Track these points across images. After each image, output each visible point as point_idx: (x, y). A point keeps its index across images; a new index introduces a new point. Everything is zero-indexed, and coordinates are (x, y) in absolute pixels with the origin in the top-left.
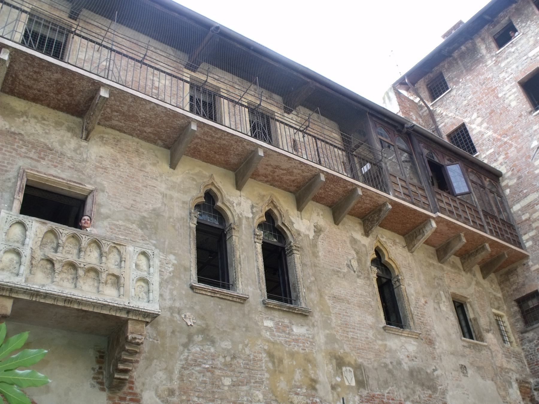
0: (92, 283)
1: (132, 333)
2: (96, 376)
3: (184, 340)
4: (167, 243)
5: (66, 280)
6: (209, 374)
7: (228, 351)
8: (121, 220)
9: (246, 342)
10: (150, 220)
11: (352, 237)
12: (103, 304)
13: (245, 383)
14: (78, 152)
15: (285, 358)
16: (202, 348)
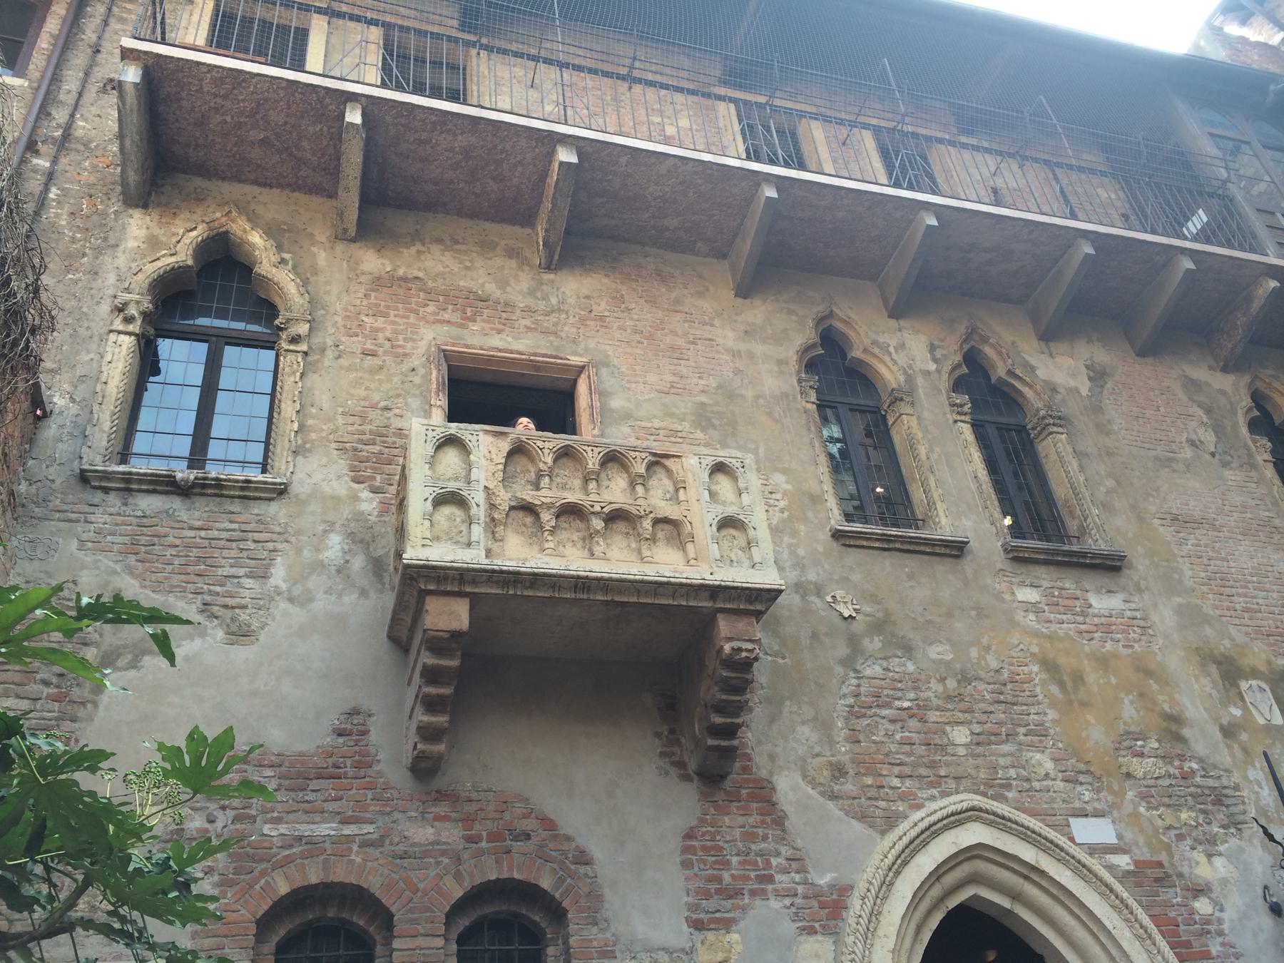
0: (625, 543)
1: (730, 639)
2: (665, 749)
3: (843, 650)
4: (762, 450)
5: (571, 544)
6: (913, 723)
7: (947, 664)
8: (655, 417)
9: (985, 641)
10: (716, 409)
11: (1186, 377)
12: (656, 583)
14: (539, 294)
15: (1088, 669)
16: (885, 665)
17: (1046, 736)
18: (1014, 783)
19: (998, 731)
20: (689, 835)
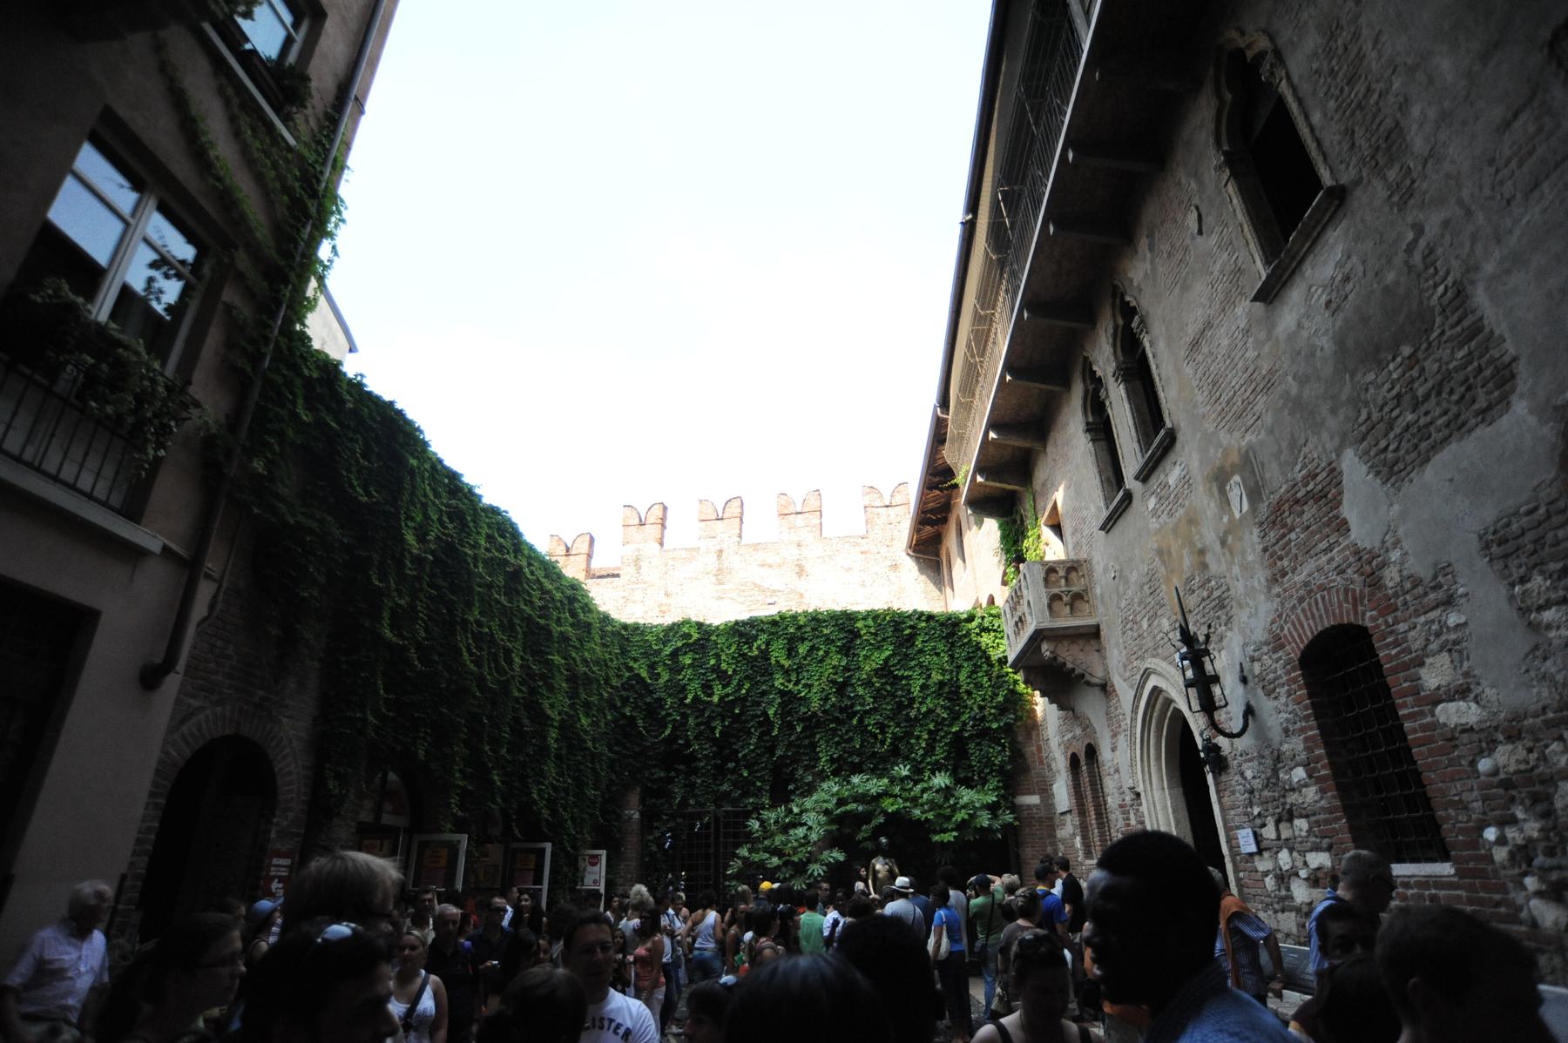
6: (1135, 627)
7: (1136, 582)
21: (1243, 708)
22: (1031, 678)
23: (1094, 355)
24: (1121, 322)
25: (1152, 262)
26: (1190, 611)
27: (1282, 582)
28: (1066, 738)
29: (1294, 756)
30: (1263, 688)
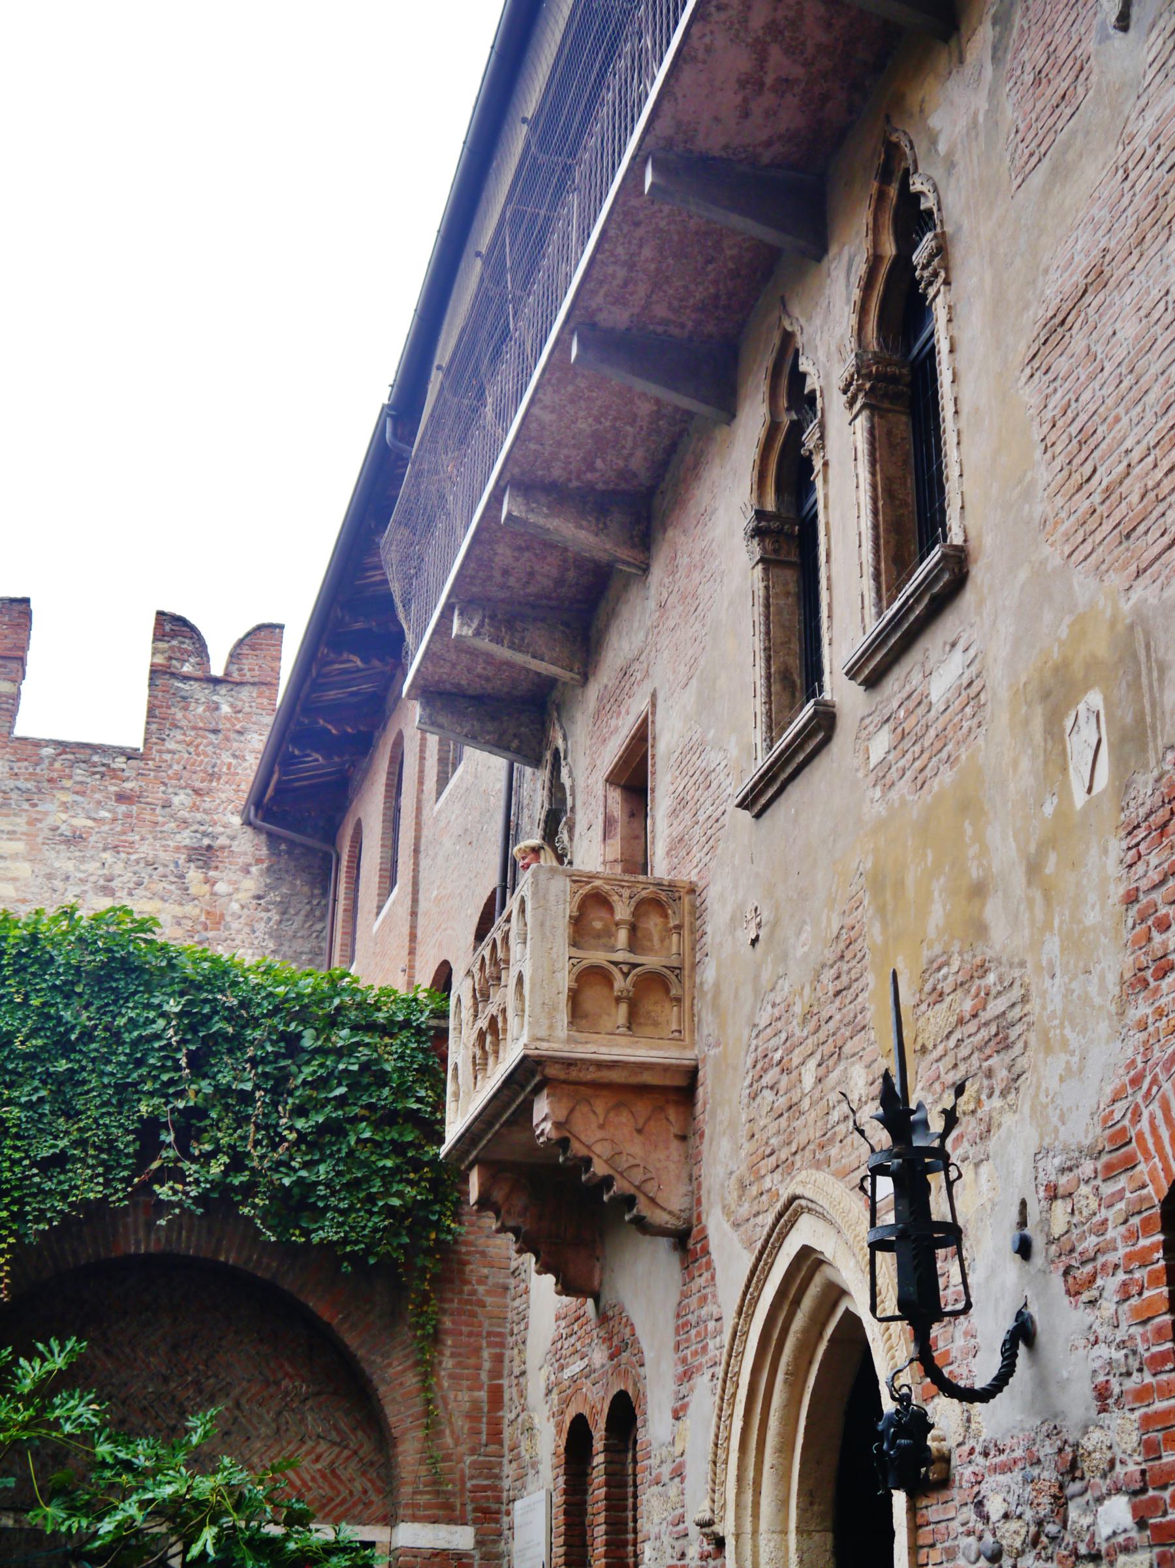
1: (537, 1125)
13: (836, 1056)
17: (864, 1027)
18: (837, 1129)
19: (832, 1049)
20: (678, 1316)
21: (1009, 1323)
22: (498, 1195)
23: (808, 330)
24: (890, 249)
25: (993, 93)
26: (924, 1050)
27: (1157, 988)
28: (567, 1373)
29: (1112, 1464)
30: (1066, 1273)
